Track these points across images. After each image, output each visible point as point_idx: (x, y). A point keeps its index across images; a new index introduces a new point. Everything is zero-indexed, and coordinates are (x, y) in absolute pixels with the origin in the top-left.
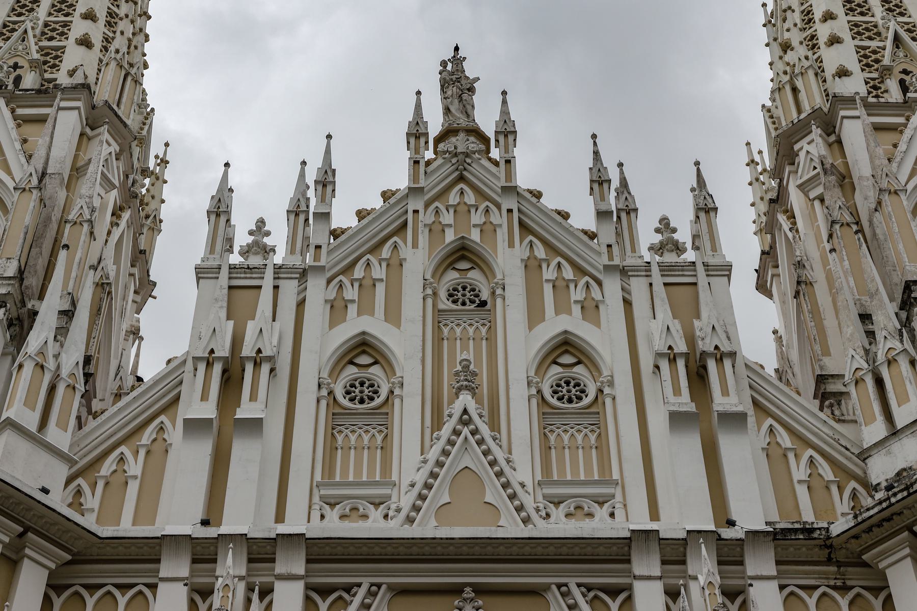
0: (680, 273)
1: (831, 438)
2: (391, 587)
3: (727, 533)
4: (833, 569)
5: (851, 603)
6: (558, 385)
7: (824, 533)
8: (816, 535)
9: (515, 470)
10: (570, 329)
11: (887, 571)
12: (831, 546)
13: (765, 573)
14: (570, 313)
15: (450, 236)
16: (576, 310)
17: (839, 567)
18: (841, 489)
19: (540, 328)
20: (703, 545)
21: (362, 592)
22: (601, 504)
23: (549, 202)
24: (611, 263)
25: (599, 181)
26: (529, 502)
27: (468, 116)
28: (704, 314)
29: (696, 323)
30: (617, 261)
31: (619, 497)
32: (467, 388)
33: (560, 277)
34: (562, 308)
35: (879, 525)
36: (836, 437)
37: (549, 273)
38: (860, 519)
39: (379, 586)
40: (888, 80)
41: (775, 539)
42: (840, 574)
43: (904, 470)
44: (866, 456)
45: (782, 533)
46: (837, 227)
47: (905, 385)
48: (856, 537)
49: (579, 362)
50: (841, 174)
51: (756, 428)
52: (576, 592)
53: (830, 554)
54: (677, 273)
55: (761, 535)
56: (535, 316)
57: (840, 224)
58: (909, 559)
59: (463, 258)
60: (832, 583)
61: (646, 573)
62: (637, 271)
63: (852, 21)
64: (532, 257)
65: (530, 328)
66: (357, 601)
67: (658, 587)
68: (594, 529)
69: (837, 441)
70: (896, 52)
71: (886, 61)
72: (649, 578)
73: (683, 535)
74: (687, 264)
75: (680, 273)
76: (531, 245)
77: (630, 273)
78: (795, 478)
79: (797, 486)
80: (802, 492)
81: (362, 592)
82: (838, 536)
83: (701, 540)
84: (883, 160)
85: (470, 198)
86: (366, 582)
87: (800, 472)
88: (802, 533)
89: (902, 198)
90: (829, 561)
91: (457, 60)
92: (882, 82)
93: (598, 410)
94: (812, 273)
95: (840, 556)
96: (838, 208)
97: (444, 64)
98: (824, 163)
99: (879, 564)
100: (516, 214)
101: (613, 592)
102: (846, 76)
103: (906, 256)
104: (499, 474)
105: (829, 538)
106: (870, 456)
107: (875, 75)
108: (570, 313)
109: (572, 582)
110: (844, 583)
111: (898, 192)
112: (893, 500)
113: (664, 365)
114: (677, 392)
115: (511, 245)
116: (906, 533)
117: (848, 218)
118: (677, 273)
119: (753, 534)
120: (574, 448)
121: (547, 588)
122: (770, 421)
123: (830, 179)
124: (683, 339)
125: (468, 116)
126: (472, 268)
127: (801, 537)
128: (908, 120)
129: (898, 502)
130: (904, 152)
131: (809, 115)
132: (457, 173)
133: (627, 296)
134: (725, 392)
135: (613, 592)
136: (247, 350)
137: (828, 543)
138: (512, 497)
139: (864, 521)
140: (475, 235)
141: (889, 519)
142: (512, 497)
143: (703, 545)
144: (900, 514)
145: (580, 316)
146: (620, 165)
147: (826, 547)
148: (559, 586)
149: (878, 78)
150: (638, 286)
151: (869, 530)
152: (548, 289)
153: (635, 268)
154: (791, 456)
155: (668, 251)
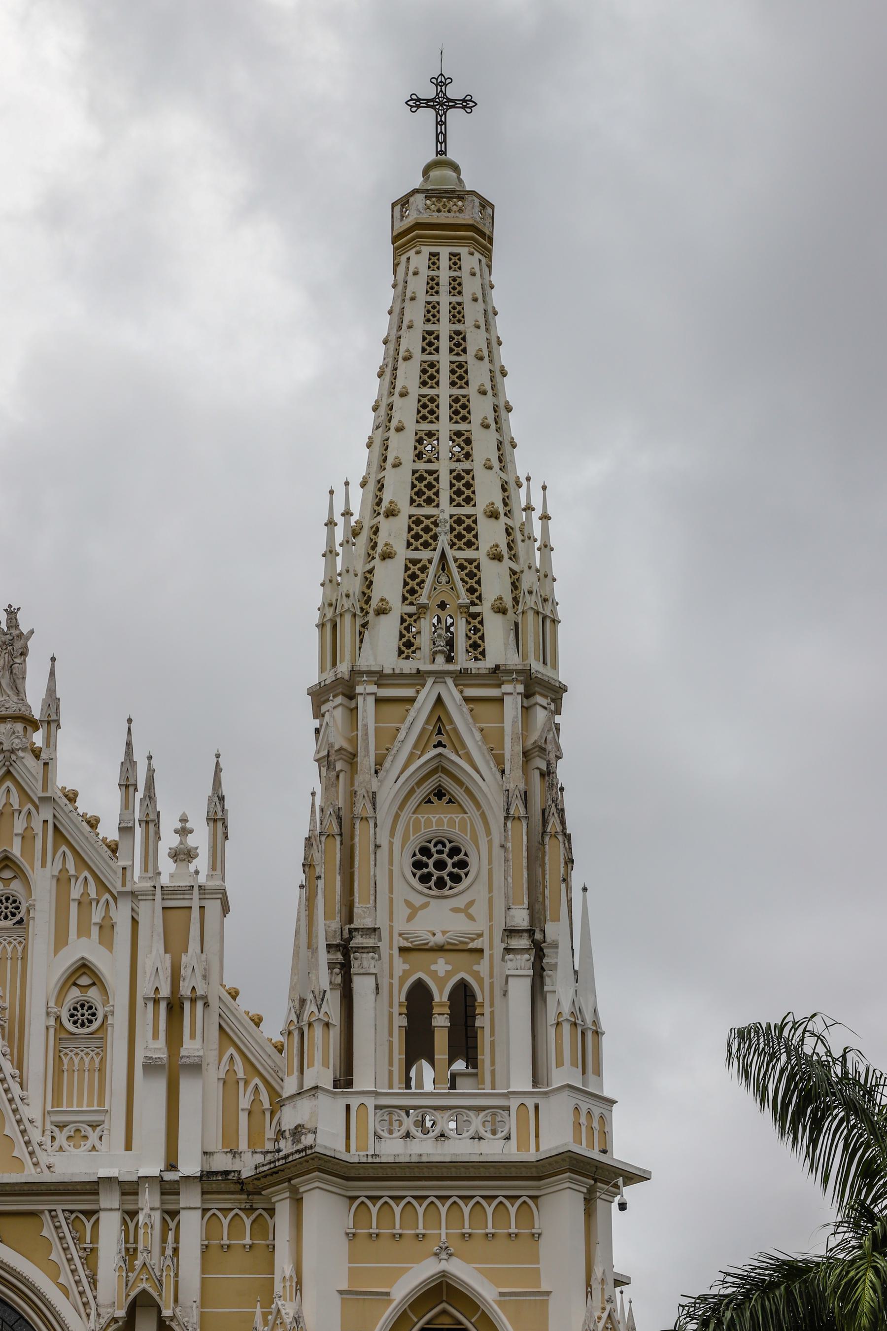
0: (182, 897)
1: (272, 1069)
3: (170, 1176)
4: (244, 1197)
5: (254, 1221)
6: (75, 1009)
7: (236, 1175)
8: (230, 1177)
9: (28, 1105)
10: (86, 956)
11: (277, 1204)
12: (242, 1183)
13: (192, 1206)
14: (89, 936)
16: (95, 931)
17: (248, 1195)
19: (63, 952)
20: (147, 1189)
23: (83, 806)
24: (124, 889)
25: (127, 786)
26: (35, 1135)
27: (18, 693)
28: (190, 950)
29: (184, 959)
30: (128, 888)
33: (85, 893)
34: (83, 931)
35: (271, 1174)
36: (276, 1069)
37: (76, 892)
38: (258, 1171)
40: (422, 620)
41: (201, 1180)
42: (249, 1200)
43: (299, 1125)
44: (282, 1104)
45: (207, 1175)
46: (323, 838)
47: (314, 1051)
48: (258, 1179)
49: (94, 984)
50: (351, 753)
51: (217, 1062)
53: (242, 1187)
54: (179, 897)
55: (191, 1179)
56: (60, 940)
57: (326, 836)
58: (288, 1201)
60: (243, 1207)
61: (109, 1207)
62: (146, 895)
63: (414, 516)
64: (64, 870)
65: (56, 952)
67: (116, 1217)
68: (72, 1174)
69: (276, 1072)
70: (439, 577)
71: (423, 600)
72: (111, 1210)
73: (136, 1179)
74: (187, 888)
75: (182, 897)
76: (64, 855)
77: (140, 897)
78: (241, 1106)
79: (240, 1113)
80: (243, 1118)
82: (245, 1178)
83: (147, 1186)
84: (367, 775)
87: (245, 1102)
88: (222, 1175)
89: (371, 826)
90: (242, 1191)
92: (419, 618)
93: (103, 1036)
94: (316, 854)
95: (250, 1188)
96: (328, 815)
98: (330, 753)
99: (272, 1198)
102: (384, 613)
103: (358, 895)
104: (15, 1111)
105: (239, 1178)
106: (284, 1105)
107: (412, 609)
108: (89, 936)
110: (251, 1206)
111: (368, 819)
113: (151, 1005)
114: (155, 1036)
115: (44, 865)
116: (286, 1184)
117: (336, 829)
118: (179, 897)
119: (187, 1178)
120: (81, 1071)
122: (232, 1050)
123: (330, 776)
124: (169, 979)
125: (18, 693)
126: (15, 877)
127: (220, 1178)
128: (418, 692)
129: (279, 1166)
130: (402, 741)
131: (332, 681)
132: (5, 769)
133: (135, 916)
134: (193, 1036)
137: (240, 1182)
138: (23, 1132)
139: (260, 1173)
141: (276, 1173)
142: (23, 1132)
143: (147, 1189)
144: (283, 1170)
145: (97, 941)
146: (150, 758)
147: (240, 1183)
149: (415, 614)
150: (144, 908)
151: (265, 1176)
152: (74, 907)
153: (144, 893)
154: (242, 1084)
155: (180, 860)
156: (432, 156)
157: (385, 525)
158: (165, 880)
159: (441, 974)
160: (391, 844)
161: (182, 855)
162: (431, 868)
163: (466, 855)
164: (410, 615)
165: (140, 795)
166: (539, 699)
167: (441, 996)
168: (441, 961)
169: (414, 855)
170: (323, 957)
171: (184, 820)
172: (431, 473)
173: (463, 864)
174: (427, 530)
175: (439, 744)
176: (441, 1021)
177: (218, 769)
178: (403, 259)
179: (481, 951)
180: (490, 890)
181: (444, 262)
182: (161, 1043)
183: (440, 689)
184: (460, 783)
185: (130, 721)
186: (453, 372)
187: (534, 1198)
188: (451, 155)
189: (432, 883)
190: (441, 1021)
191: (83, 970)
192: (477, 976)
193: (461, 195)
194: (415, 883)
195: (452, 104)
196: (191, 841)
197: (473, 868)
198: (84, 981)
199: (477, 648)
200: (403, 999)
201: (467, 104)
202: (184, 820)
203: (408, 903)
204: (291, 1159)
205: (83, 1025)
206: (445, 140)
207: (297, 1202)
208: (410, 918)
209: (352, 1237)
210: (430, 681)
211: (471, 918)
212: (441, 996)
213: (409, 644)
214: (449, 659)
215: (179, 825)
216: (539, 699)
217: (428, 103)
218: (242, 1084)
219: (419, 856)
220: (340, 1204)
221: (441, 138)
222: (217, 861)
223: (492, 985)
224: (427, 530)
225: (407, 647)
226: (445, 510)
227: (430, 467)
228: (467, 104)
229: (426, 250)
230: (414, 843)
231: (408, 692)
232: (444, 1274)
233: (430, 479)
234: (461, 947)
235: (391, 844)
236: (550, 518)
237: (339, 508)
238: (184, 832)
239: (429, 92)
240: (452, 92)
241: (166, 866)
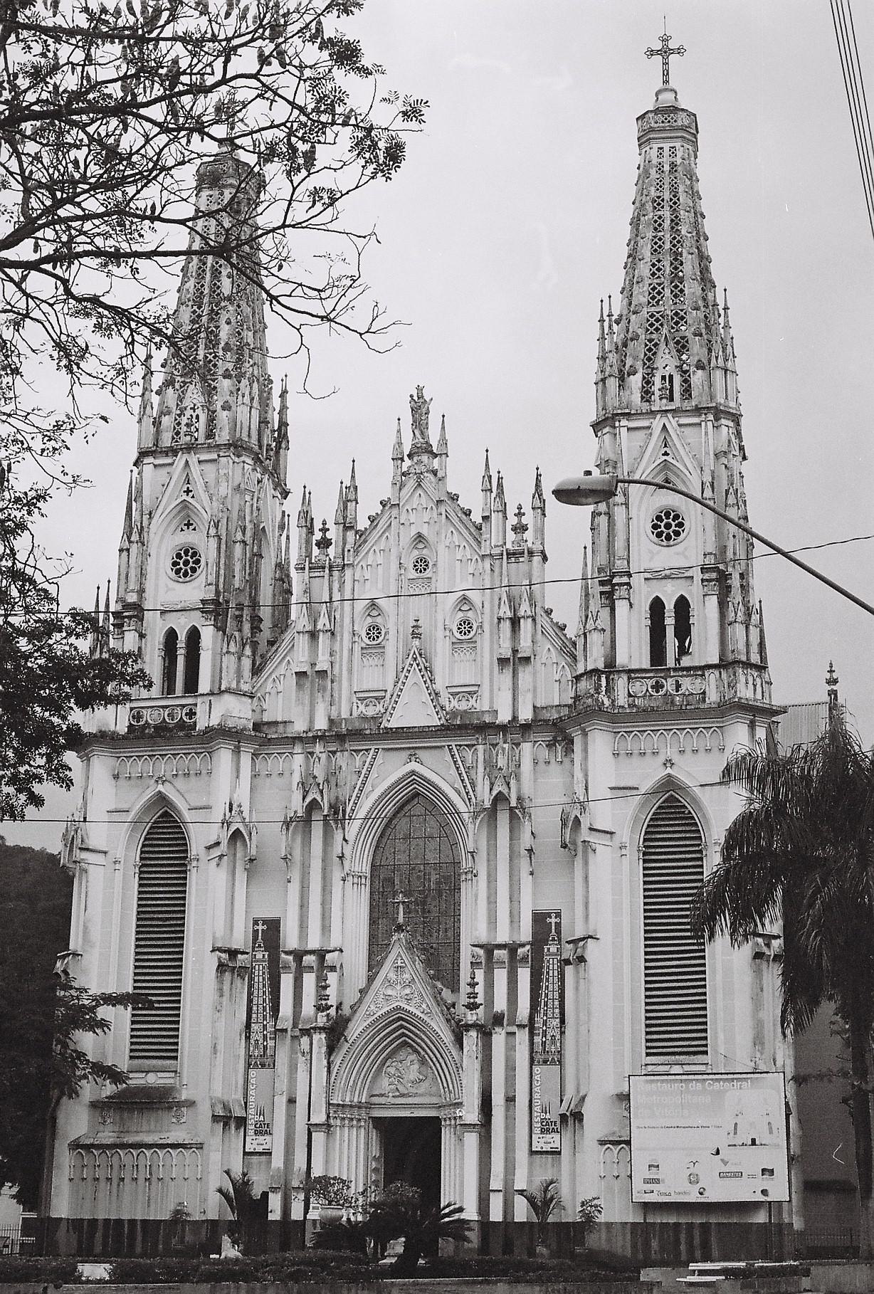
15: (413, 532)
21: (372, 750)
59: (420, 541)
66: (370, 756)
81: (372, 750)
85: (424, 500)
86: (373, 748)
91: (419, 389)
97: (411, 396)
100: (444, 513)
109: (453, 744)
136: (320, 626)
140: (425, 532)
148: (448, 746)
156: (660, 85)
157: (633, 317)
158: (509, 546)
159: (669, 592)
160: (638, 515)
161: (520, 529)
162: (663, 529)
163: (683, 519)
164: (648, 374)
165: (494, 495)
166: (723, 421)
167: (670, 606)
168: (669, 585)
169: (653, 521)
170: (596, 589)
171: (520, 508)
172: (659, 284)
173: (681, 525)
174: (657, 320)
175: (666, 454)
176: (670, 621)
177: (539, 476)
178: (644, 150)
180: (697, 540)
181: (666, 152)
183: (664, 420)
184: (678, 476)
185: (487, 451)
186: (672, 220)
188: (672, 84)
189: (663, 538)
190: (670, 621)
191: (464, 601)
192: (690, 593)
193: (675, 109)
194: (654, 538)
195: (672, 51)
196: (524, 520)
197: (686, 524)
198: (465, 607)
199: (687, 392)
200: (648, 609)
201: (680, 51)
202: (520, 508)
203: (651, 552)
205: (465, 634)
206: (668, 74)
207: (585, 734)
208: (651, 559)
209: (616, 755)
210: (659, 416)
211: (686, 557)
212: (670, 606)
213: (647, 392)
214: (671, 399)
215: (517, 511)
216: (723, 421)
217: (658, 52)
218: (555, 665)
219: (656, 521)
220: (609, 736)
221: (666, 74)
222: (540, 532)
224: (657, 320)
225: (646, 394)
226: (667, 307)
227: (658, 281)
228: (680, 51)
229: (656, 146)
230: (652, 514)
231: (645, 423)
232: (669, 775)
233: (659, 288)
235: (638, 515)
236: (728, 309)
237: (606, 313)
238: (520, 514)
239: (658, 46)
240: (672, 45)
241: (511, 536)
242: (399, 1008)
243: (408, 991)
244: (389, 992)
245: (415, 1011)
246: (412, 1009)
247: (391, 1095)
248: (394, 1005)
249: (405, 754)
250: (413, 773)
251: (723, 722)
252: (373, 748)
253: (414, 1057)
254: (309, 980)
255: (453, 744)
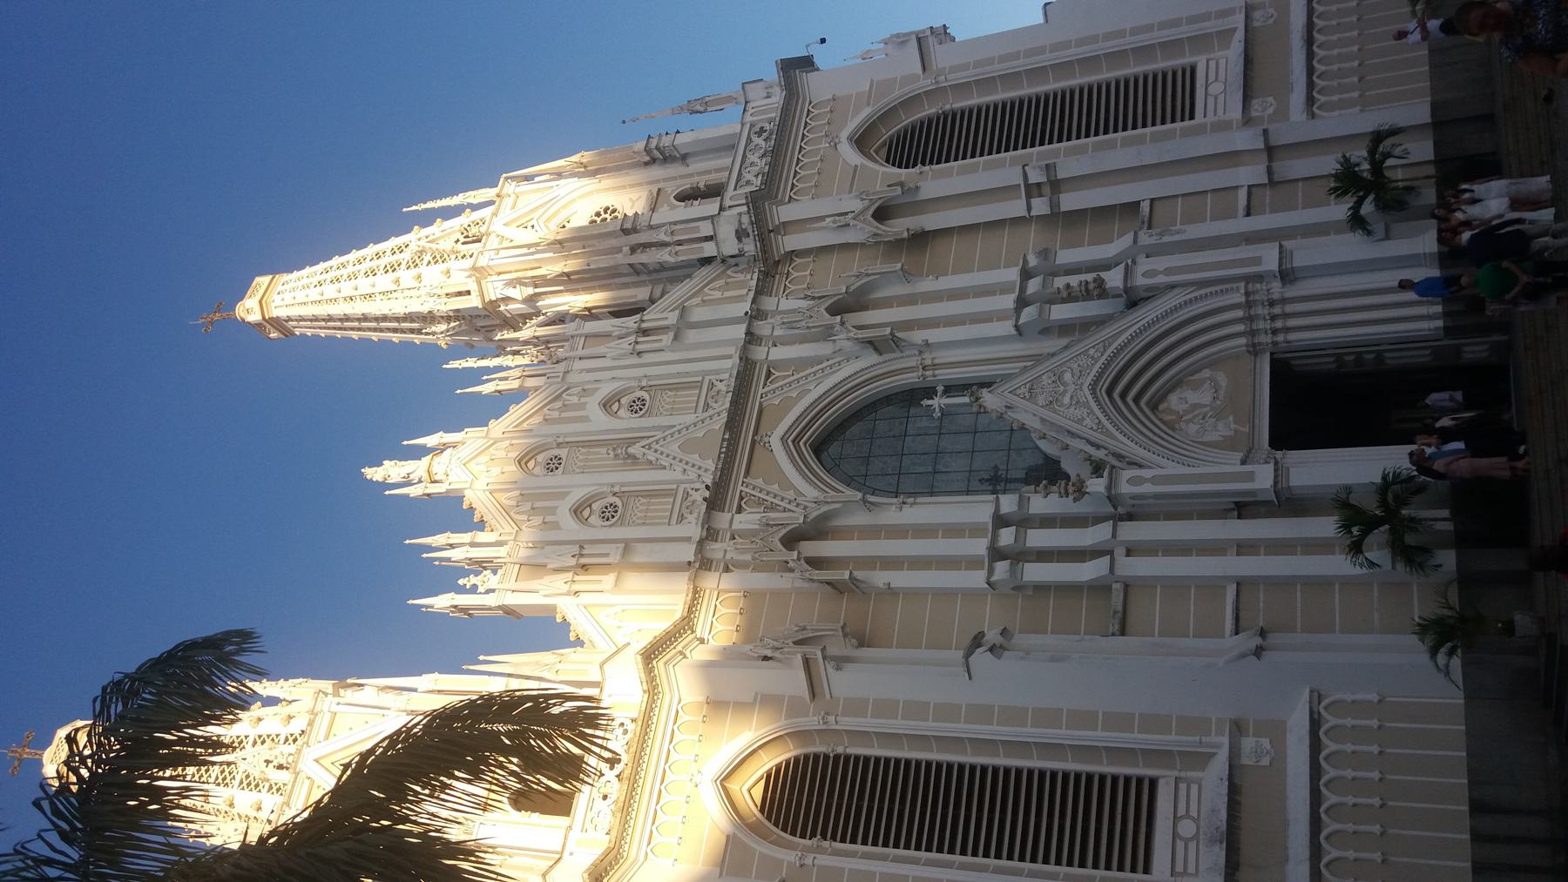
2: (745, 477)
4: (778, 276)
8: (761, 277)
16: (583, 400)
18: (730, 277)
22: (712, 385)
30: (561, 375)
31: (713, 378)
32: (627, 448)
39: (743, 482)
52: (766, 389)
56: (585, 419)
67: (773, 350)
72: (768, 352)
79: (724, 296)
87: (717, 294)
101: (769, 374)
108: (586, 403)
112: (756, 233)
121: (761, 403)
135: (769, 374)
148: (762, 397)
179: (659, 190)
182: (664, 337)
187: (810, 103)
204: (753, 219)
223: (682, 177)
232: (850, 139)
234: (655, 199)
242: (1093, 387)
243: (1067, 376)
244: (1067, 400)
245: (1099, 364)
246: (1096, 368)
247: (1232, 426)
248: (1087, 393)
249: (758, 449)
250: (783, 439)
251: (804, 99)
252: (740, 488)
253: (1174, 401)
254: (1038, 538)
255: (761, 391)
